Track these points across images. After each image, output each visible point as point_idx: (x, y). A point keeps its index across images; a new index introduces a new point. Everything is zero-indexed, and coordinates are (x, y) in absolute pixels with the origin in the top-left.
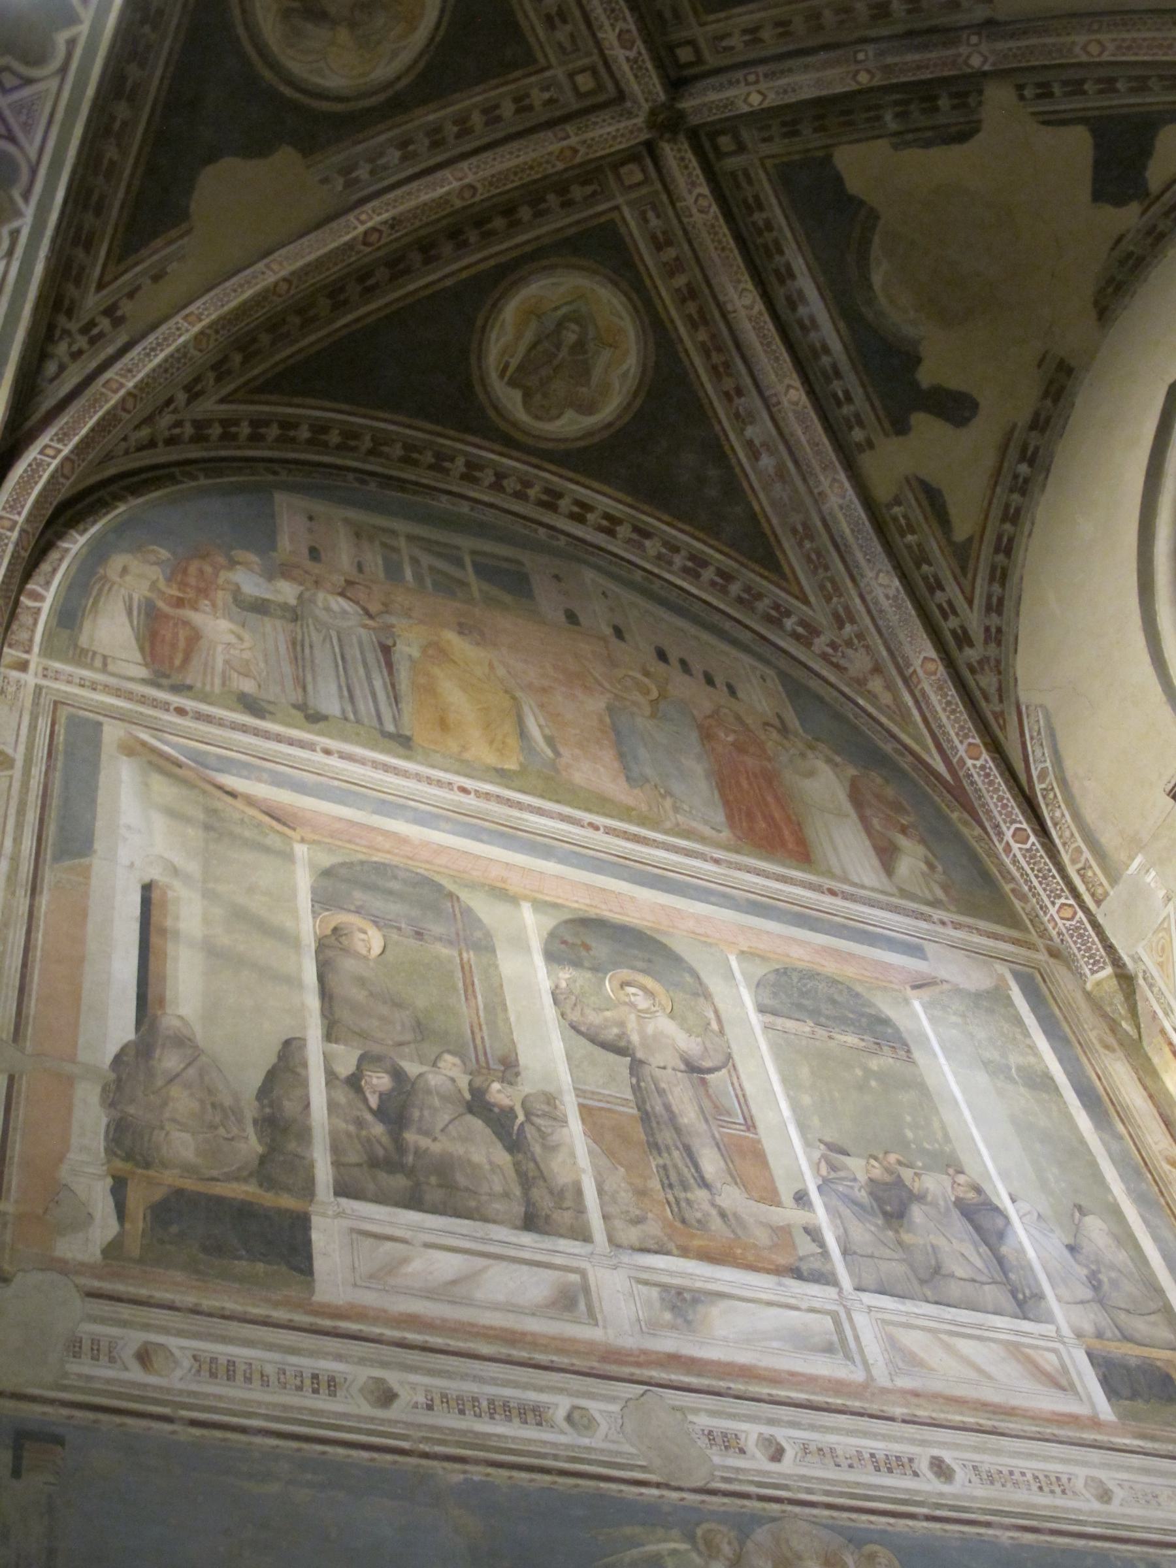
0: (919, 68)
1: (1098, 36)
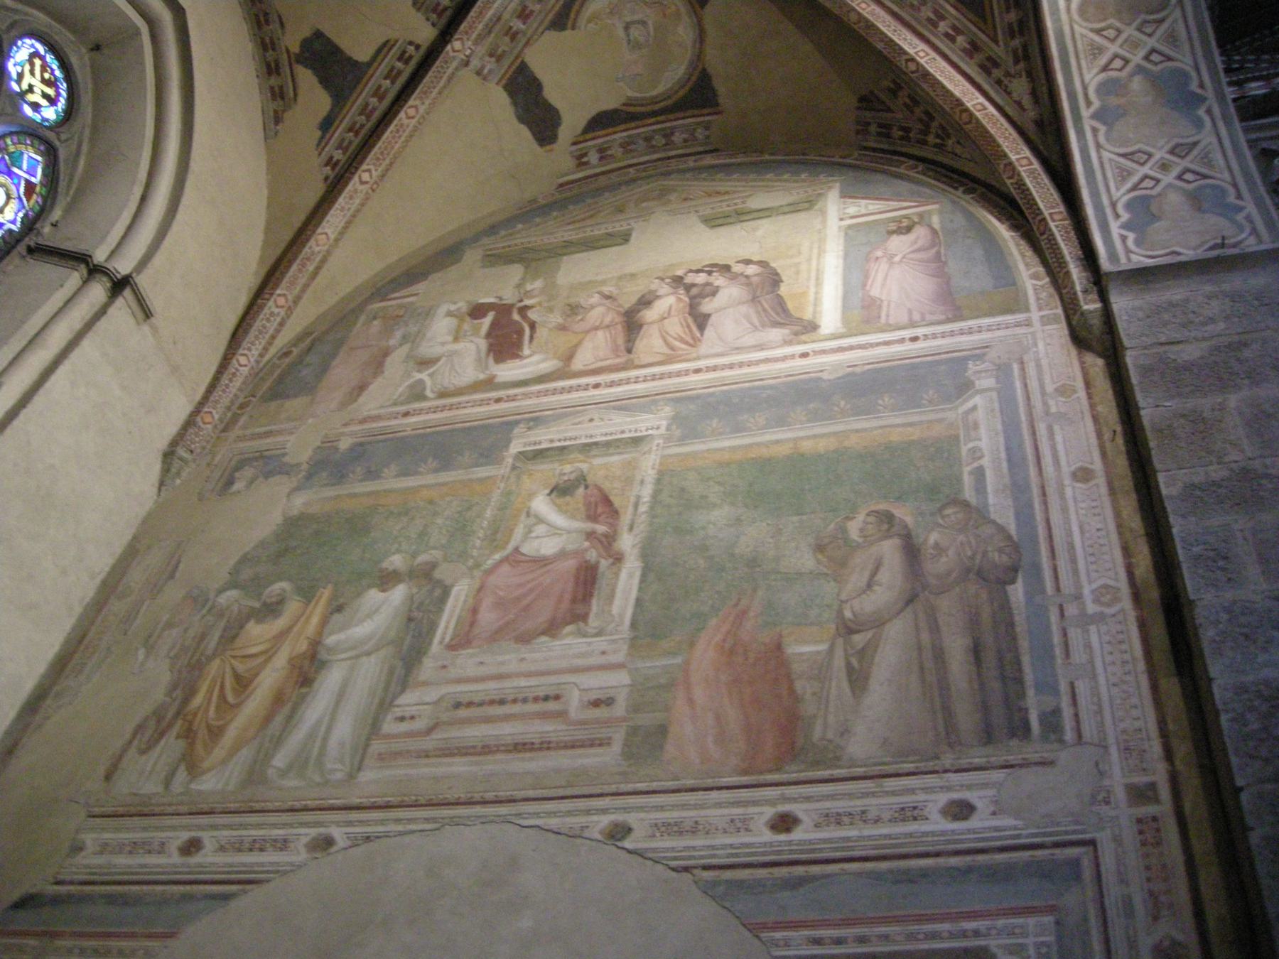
0: (481, 13)
1: (416, 119)
